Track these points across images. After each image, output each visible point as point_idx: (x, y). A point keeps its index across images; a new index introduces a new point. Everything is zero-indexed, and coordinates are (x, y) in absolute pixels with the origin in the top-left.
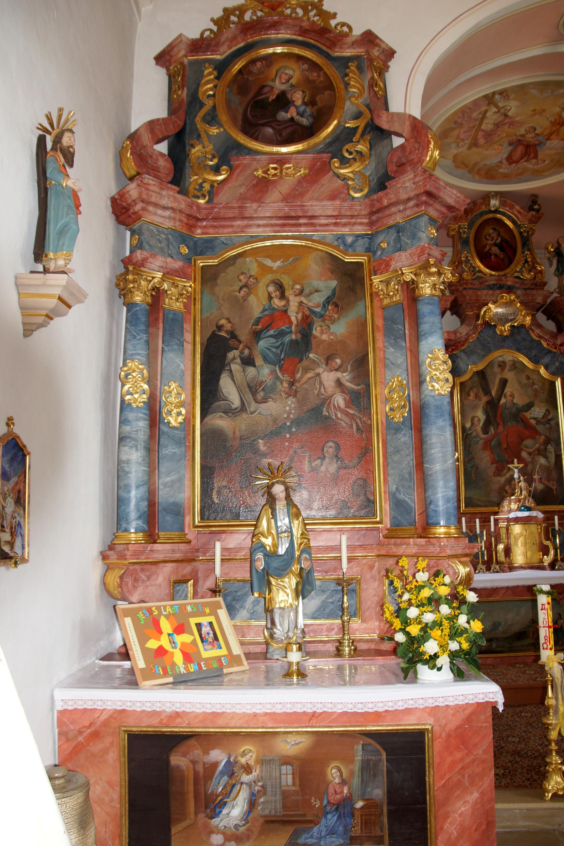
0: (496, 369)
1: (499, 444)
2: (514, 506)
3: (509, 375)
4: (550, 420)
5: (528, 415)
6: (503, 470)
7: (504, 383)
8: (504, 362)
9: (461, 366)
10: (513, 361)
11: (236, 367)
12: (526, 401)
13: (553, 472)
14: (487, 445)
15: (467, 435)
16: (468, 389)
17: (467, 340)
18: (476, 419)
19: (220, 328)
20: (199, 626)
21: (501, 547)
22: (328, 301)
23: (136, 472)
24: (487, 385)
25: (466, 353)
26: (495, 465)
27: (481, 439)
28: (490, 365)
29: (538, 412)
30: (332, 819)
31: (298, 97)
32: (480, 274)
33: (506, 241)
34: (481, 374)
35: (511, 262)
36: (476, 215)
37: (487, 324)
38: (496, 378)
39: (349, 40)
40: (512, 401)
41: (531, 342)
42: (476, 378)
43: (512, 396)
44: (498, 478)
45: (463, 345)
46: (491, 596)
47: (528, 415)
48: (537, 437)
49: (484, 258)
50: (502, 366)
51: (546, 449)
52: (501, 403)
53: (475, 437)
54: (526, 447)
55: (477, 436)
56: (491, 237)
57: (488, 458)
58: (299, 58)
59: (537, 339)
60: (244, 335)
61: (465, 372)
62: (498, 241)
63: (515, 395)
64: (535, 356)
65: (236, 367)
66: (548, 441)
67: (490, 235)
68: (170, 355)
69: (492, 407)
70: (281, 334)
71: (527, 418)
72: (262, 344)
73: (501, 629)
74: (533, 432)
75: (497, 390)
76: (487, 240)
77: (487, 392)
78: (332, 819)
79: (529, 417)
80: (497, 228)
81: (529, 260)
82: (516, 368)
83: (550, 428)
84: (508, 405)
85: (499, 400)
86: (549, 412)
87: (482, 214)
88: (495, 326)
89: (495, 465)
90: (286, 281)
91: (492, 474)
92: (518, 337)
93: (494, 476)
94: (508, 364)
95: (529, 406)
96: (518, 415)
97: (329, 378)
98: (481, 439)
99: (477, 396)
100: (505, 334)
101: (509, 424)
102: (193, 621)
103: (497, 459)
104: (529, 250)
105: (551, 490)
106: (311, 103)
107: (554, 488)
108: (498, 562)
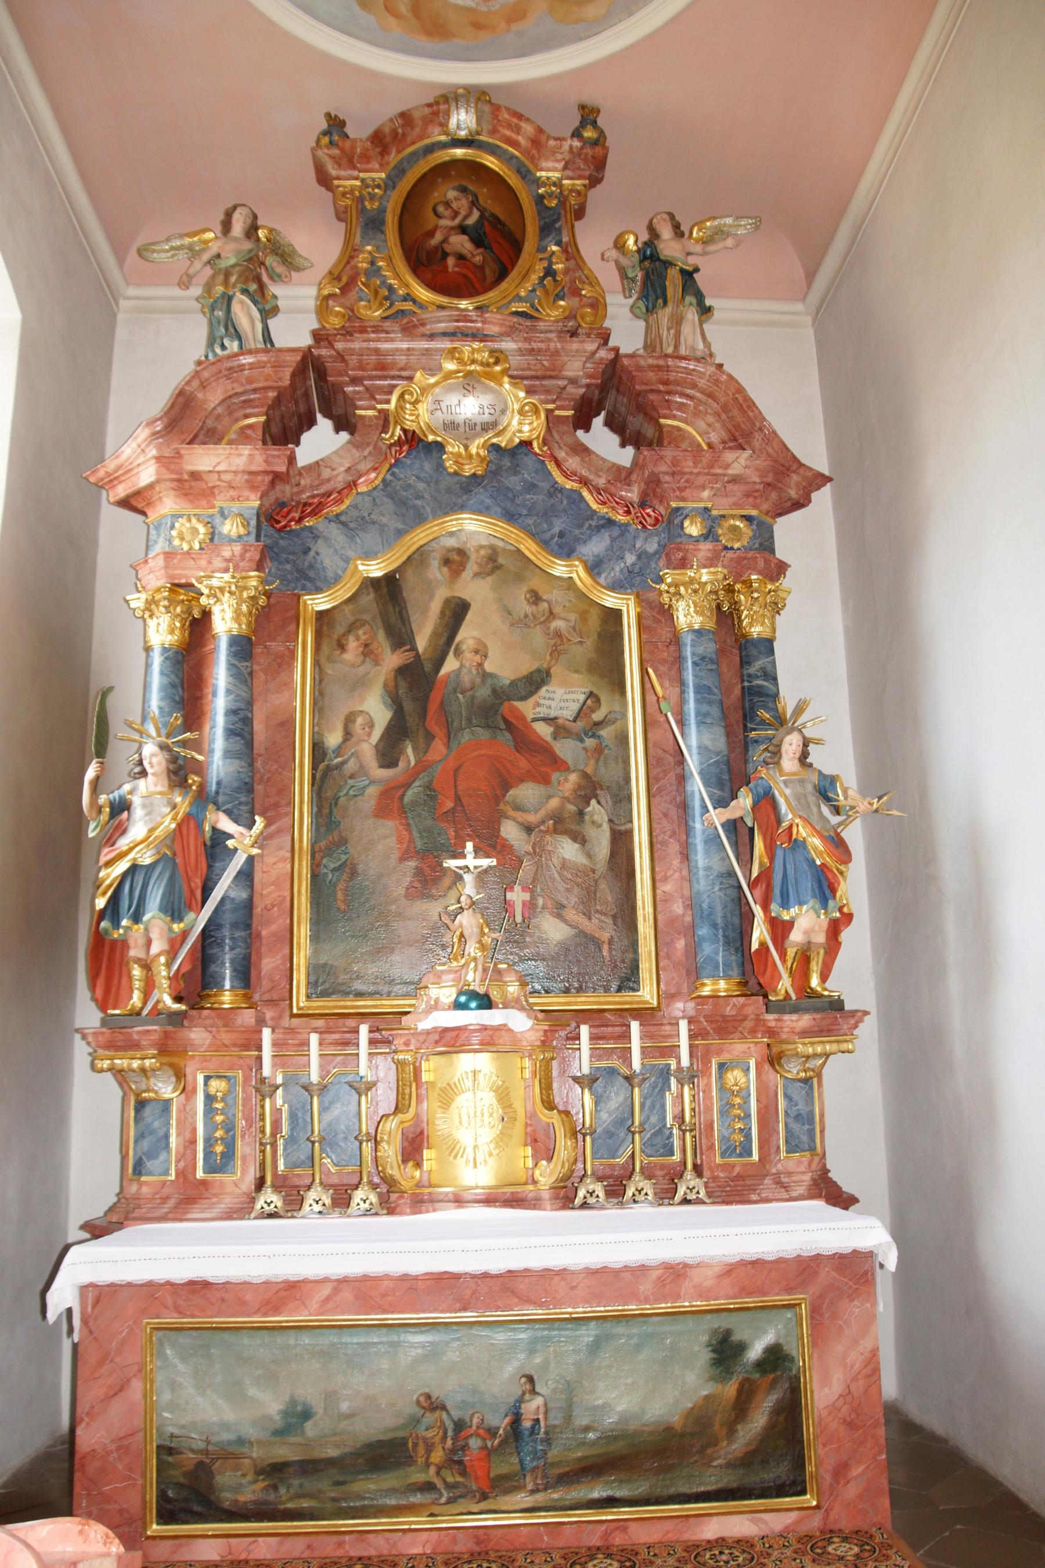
0: (436, 571)
1: (431, 793)
2: (447, 994)
4: (598, 724)
5: (527, 708)
6: (436, 880)
7: (457, 612)
8: (461, 552)
9: (327, 562)
10: (493, 549)
13: (603, 886)
15: (328, 769)
16: (340, 630)
17: (352, 485)
18: (360, 721)
24: (404, 618)
25: (342, 523)
26: (412, 864)
27: (372, 782)
28: (418, 558)
29: (561, 698)
32: (408, 306)
33: (496, 221)
34: (389, 588)
35: (502, 274)
36: (413, 154)
37: (412, 440)
38: (431, 597)
40: (480, 665)
41: (551, 495)
42: (368, 598)
43: (481, 651)
44: (421, 906)
45: (340, 501)
46: (276, 1310)
47: (527, 708)
48: (555, 776)
49: (425, 261)
50: (455, 561)
51: (581, 813)
52: (443, 671)
53: (352, 777)
54: (518, 808)
55: (362, 770)
56: (453, 210)
57: (392, 841)
59: (569, 485)
61: (337, 579)
62: (471, 221)
63: (490, 647)
64: (561, 535)
66: (589, 789)
67: (447, 204)
71: (523, 718)
73: (310, 1429)
74: (543, 762)
75: (435, 635)
76: (439, 216)
77: (401, 638)
79: (530, 716)
80: (470, 187)
81: (559, 267)
82: (498, 567)
83: (599, 750)
84: (466, 679)
86: (598, 701)
87: (430, 149)
88: (440, 447)
89: (412, 864)
91: (402, 891)
92: (513, 482)
93: (407, 896)
94: (473, 557)
95: (534, 682)
96: (496, 710)
98: (372, 782)
99: (367, 651)
100: (468, 470)
101: (466, 737)
103: (419, 844)
104: (559, 243)
105: (598, 944)
107: (605, 936)
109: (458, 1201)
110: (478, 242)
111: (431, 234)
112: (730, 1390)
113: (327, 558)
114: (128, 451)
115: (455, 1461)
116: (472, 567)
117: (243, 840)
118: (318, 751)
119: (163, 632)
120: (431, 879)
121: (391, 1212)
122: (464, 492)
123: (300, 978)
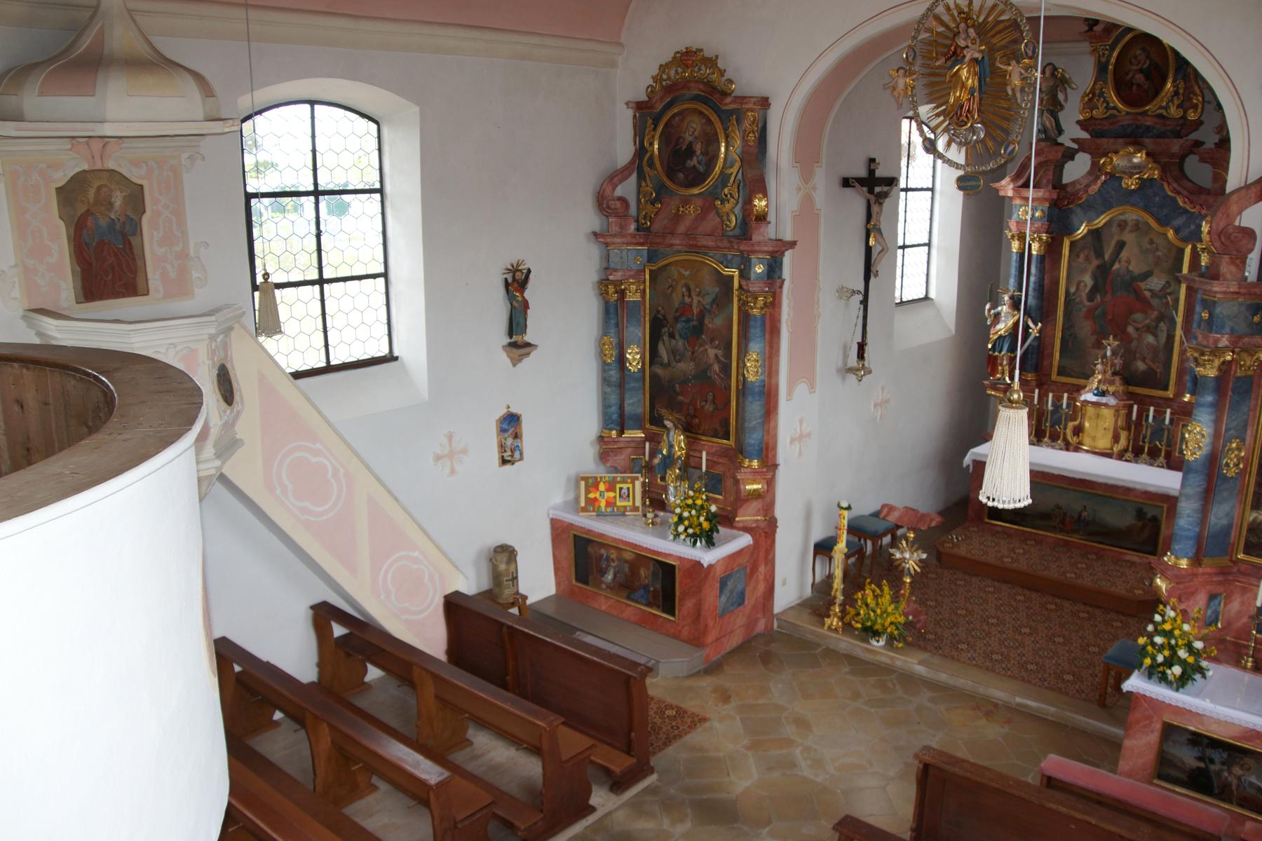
0: (1115, 229)
3: (1128, 237)
5: (1143, 285)
7: (1121, 245)
8: (1125, 221)
11: (666, 338)
12: (1145, 268)
14: (1090, 314)
19: (658, 312)
20: (621, 489)
21: (1071, 425)
22: (714, 301)
23: (614, 399)
24: (1101, 248)
29: (1156, 283)
30: (642, 591)
31: (698, 148)
32: (1115, 112)
34: (1095, 234)
39: (728, 100)
43: (1128, 262)
47: (1143, 285)
50: (1122, 225)
51: (1156, 327)
55: (1081, 302)
58: (701, 113)
60: (670, 318)
63: (1132, 260)
65: (666, 338)
68: (631, 329)
69: (1103, 273)
70: (687, 321)
72: (679, 326)
77: (1099, 255)
78: (642, 591)
85: (1112, 265)
88: (1121, 178)
90: (692, 286)
95: (1146, 275)
96: (1131, 284)
97: (712, 352)
99: (1087, 259)
102: (618, 486)
105: (1155, 373)
106: (705, 153)
108: (1065, 440)
109: (1087, 451)
110: (1147, 78)
111: (1127, 74)
112: (1140, 524)
113: (1075, 220)
114: (1003, 182)
115: (1063, 522)
116: (1128, 228)
117: (1035, 330)
118: (1067, 292)
119: (1015, 245)
120: (1099, 345)
121: (1067, 450)
122: (1127, 197)
123: (1055, 370)
